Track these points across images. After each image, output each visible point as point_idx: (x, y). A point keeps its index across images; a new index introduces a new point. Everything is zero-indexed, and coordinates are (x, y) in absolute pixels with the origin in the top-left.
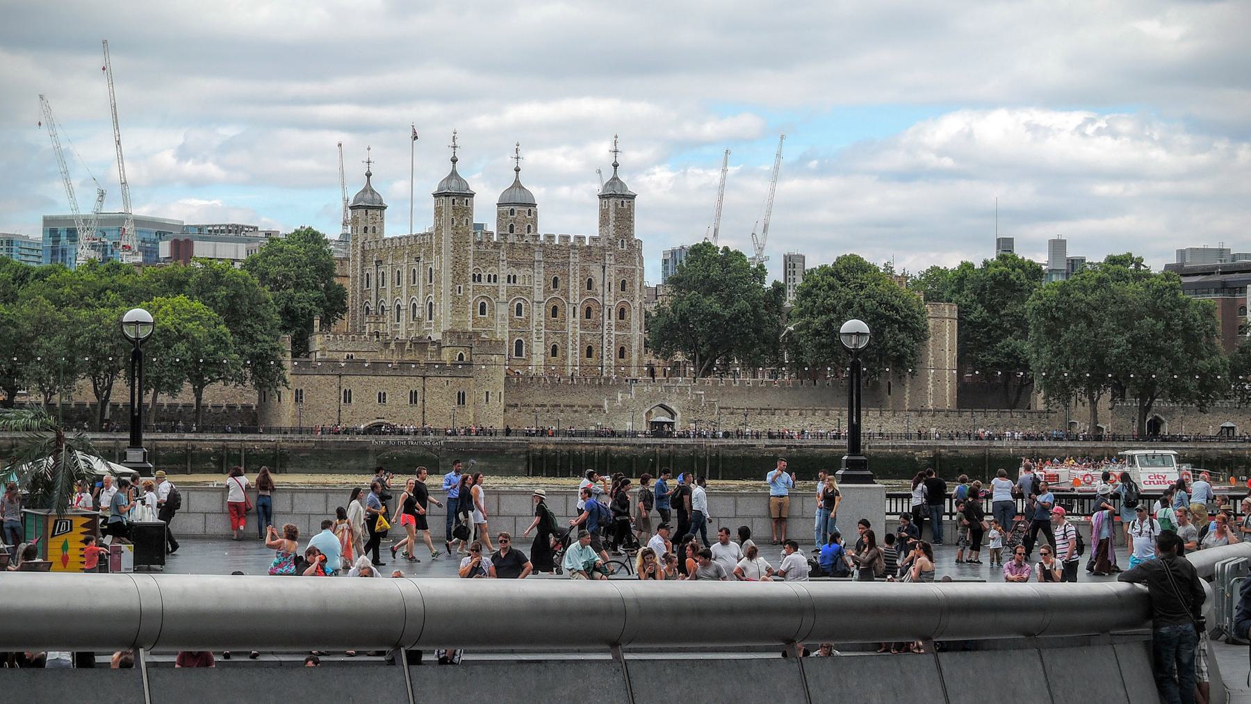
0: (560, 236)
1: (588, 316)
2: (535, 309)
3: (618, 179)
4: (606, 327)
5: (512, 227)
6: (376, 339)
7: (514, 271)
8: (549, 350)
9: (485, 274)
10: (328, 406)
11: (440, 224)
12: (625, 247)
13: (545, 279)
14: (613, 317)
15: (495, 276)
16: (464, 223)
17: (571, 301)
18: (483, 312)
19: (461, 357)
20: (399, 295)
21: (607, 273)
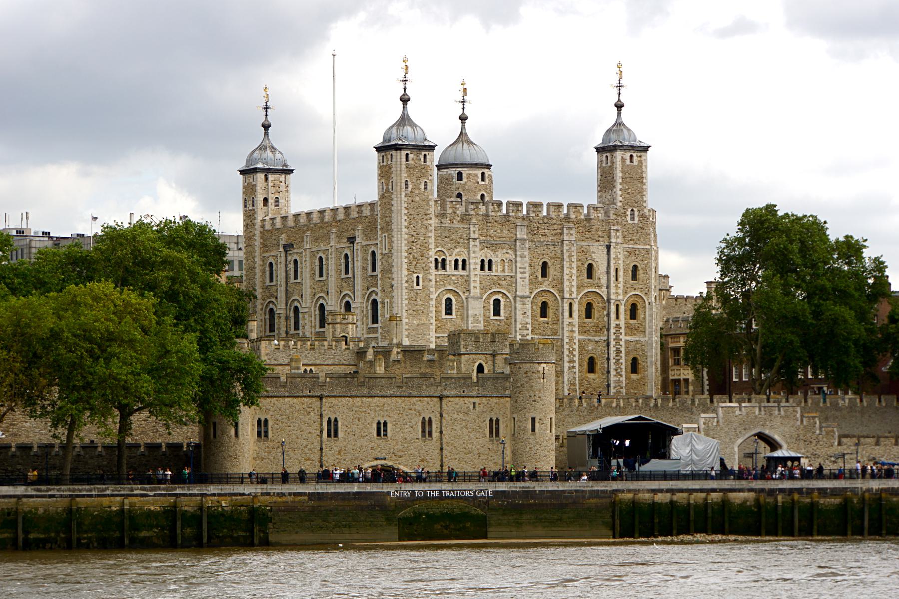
0: (549, 205)
1: (589, 315)
2: (519, 306)
3: (624, 125)
4: (613, 331)
5: (460, 196)
6: (344, 347)
7: (488, 254)
10: (305, 443)
11: (387, 190)
15: (464, 261)
16: (422, 186)
17: (567, 295)
18: (449, 311)
19: (481, 369)
20: (322, 291)
21: (613, 256)
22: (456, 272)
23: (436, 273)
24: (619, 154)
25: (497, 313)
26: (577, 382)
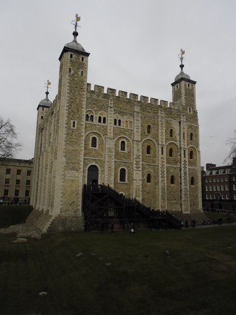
1: (171, 155)
2: (135, 146)
3: (183, 73)
4: (183, 163)
7: (120, 117)
8: (145, 177)
9: (96, 115)
11: (62, 76)
12: (192, 113)
13: (142, 126)
14: (187, 156)
15: (104, 118)
16: (80, 73)
17: (160, 143)
18: (94, 144)
21: (182, 127)
22: (99, 124)
23: (87, 122)
24: (183, 83)
25: (123, 148)
26: (166, 188)
